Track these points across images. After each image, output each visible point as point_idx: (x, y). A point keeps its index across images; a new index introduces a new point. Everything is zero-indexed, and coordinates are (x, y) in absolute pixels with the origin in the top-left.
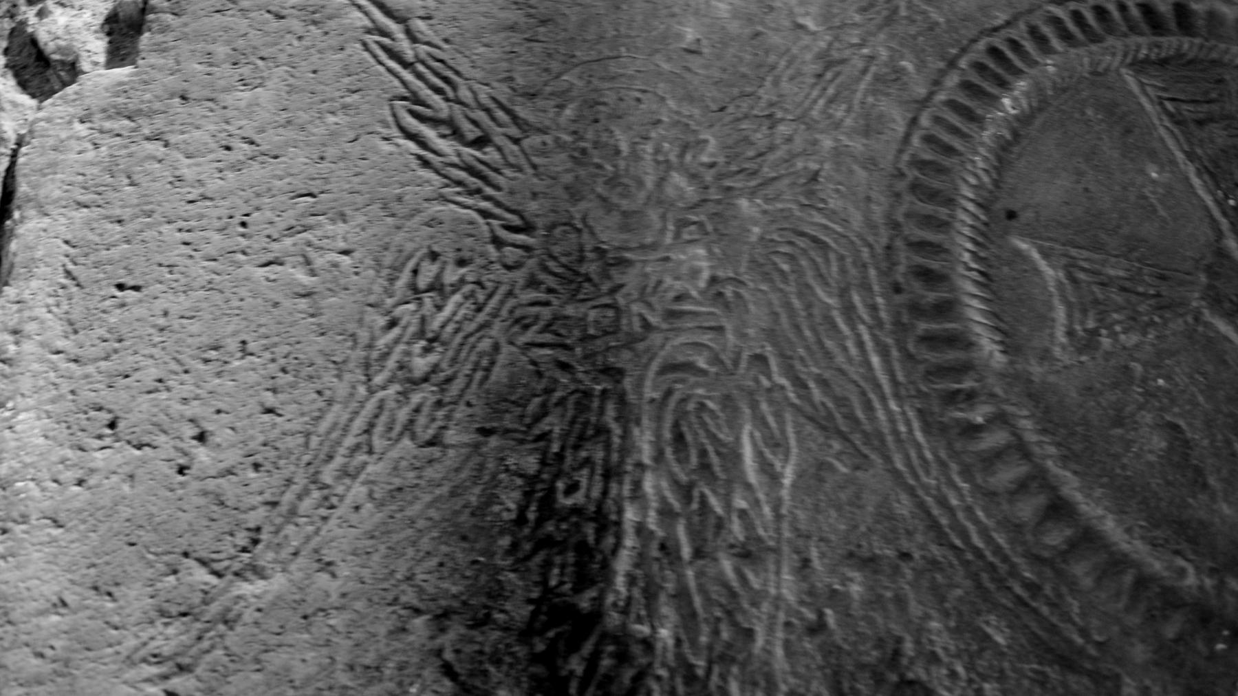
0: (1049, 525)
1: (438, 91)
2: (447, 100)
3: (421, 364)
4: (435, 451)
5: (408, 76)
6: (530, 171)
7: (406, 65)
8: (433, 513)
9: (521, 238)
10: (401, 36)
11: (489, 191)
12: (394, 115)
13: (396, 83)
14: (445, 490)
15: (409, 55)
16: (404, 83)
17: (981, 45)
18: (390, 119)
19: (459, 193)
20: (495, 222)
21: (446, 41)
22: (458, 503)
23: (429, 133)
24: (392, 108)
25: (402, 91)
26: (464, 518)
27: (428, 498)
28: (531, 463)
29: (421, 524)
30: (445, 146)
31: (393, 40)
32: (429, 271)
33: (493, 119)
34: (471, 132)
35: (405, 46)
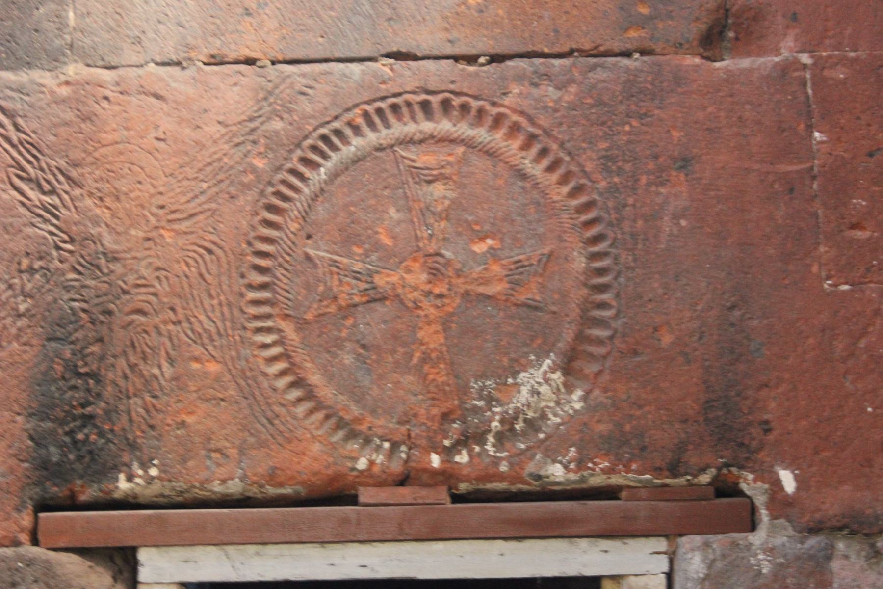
0: (293, 389)
1: (29, 162)
2: (34, 168)
3: (22, 308)
4: (27, 348)
5: (15, 154)
6: (73, 209)
7: (13, 146)
8: (26, 375)
9: (68, 247)
10: (11, 127)
11: (55, 221)
12: (9, 177)
13: (10, 159)
14: (31, 364)
15: (15, 140)
16: (13, 158)
17: (315, 135)
18: (6, 179)
19: (39, 222)
20: (56, 238)
21: (34, 132)
22: (36, 370)
23: (24, 187)
24: (7, 172)
25: (13, 163)
26: (40, 376)
27: (23, 368)
28: (68, 355)
29: (21, 378)
30: (33, 195)
31: (6, 130)
32: (25, 262)
33: (57, 180)
34: (47, 187)
35: (14, 136)
